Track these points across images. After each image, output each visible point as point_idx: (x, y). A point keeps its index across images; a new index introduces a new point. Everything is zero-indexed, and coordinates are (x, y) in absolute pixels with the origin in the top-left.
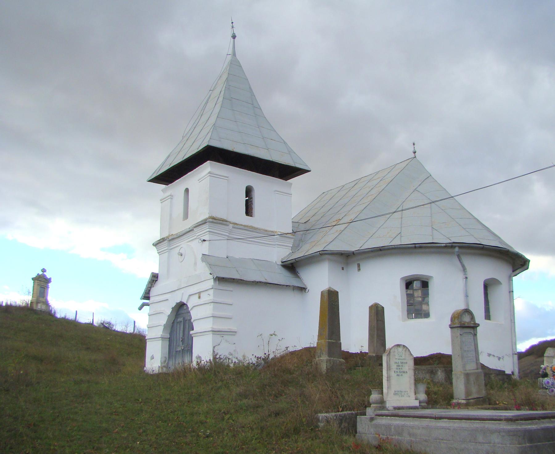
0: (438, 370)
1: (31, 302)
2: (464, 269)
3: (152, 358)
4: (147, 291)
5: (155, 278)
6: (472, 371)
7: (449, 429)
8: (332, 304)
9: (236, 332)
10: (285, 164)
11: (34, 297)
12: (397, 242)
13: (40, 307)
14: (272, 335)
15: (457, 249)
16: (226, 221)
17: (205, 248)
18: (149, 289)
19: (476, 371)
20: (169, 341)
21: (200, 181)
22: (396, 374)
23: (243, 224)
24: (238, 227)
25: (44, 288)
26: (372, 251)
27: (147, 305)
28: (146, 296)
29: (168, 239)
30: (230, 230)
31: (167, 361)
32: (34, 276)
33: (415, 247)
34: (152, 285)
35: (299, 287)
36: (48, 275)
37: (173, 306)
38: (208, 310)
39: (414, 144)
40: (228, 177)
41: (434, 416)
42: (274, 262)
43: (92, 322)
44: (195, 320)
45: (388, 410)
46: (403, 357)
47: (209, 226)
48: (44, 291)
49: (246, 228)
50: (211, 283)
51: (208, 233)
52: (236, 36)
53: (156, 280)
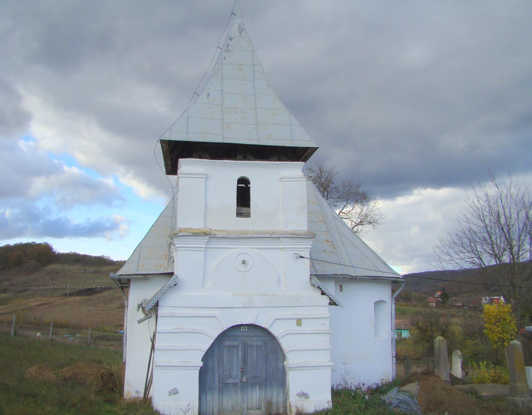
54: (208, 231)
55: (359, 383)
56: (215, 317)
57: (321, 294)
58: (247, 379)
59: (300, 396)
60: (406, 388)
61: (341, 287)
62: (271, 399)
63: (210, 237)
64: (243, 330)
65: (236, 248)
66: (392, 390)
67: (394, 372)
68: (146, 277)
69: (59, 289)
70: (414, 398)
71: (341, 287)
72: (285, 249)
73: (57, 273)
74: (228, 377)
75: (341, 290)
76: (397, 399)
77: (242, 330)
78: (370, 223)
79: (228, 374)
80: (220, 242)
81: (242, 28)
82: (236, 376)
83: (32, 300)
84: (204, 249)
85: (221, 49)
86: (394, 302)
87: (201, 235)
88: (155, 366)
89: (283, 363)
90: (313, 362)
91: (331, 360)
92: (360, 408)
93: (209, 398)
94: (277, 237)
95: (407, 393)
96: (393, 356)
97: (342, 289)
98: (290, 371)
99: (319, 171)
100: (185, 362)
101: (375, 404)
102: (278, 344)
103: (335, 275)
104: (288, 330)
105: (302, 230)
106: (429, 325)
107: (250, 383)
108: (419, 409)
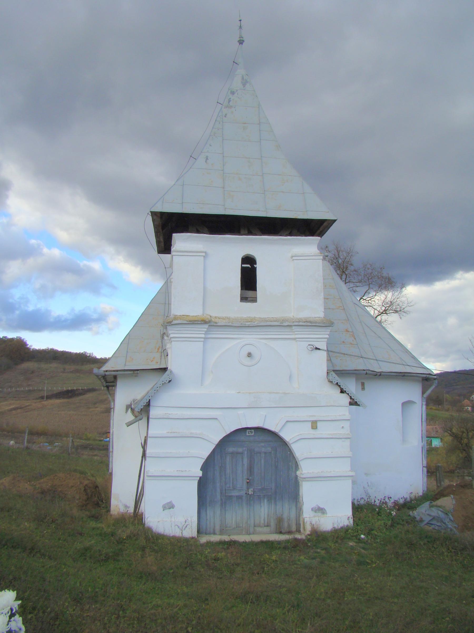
54: (208, 318)
55: (385, 497)
56: (216, 419)
57: (340, 392)
58: (254, 492)
59: (315, 511)
60: (440, 502)
61: (363, 384)
62: (282, 515)
63: (209, 326)
64: (249, 434)
65: (240, 338)
66: (423, 505)
67: (424, 485)
68: (135, 373)
69: (34, 391)
70: (448, 514)
71: (363, 384)
72: (297, 340)
73: (33, 372)
74: (231, 488)
75: (363, 389)
76: (428, 515)
77: (247, 434)
78: (396, 312)
79: (231, 485)
81: (246, 79)
82: (241, 487)
83: (4, 403)
84: (203, 340)
85: (222, 104)
86: (425, 402)
87: (199, 323)
88: (147, 476)
89: (295, 473)
90: (331, 472)
91: (352, 470)
92: (386, 525)
93: (210, 512)
94: (288, 326)
95: (441, 508)
96: (423, 466)
97: (364, 387)
98: (304, 482)
99: (336, 251)
100: (182, 471)
101: (403, 521)
102: (290, 450)
103: (356, 370)
104: (301, 434)
105: (318, 317)
106: (465, 430)
107: (258, 495)
108: (455, 527)
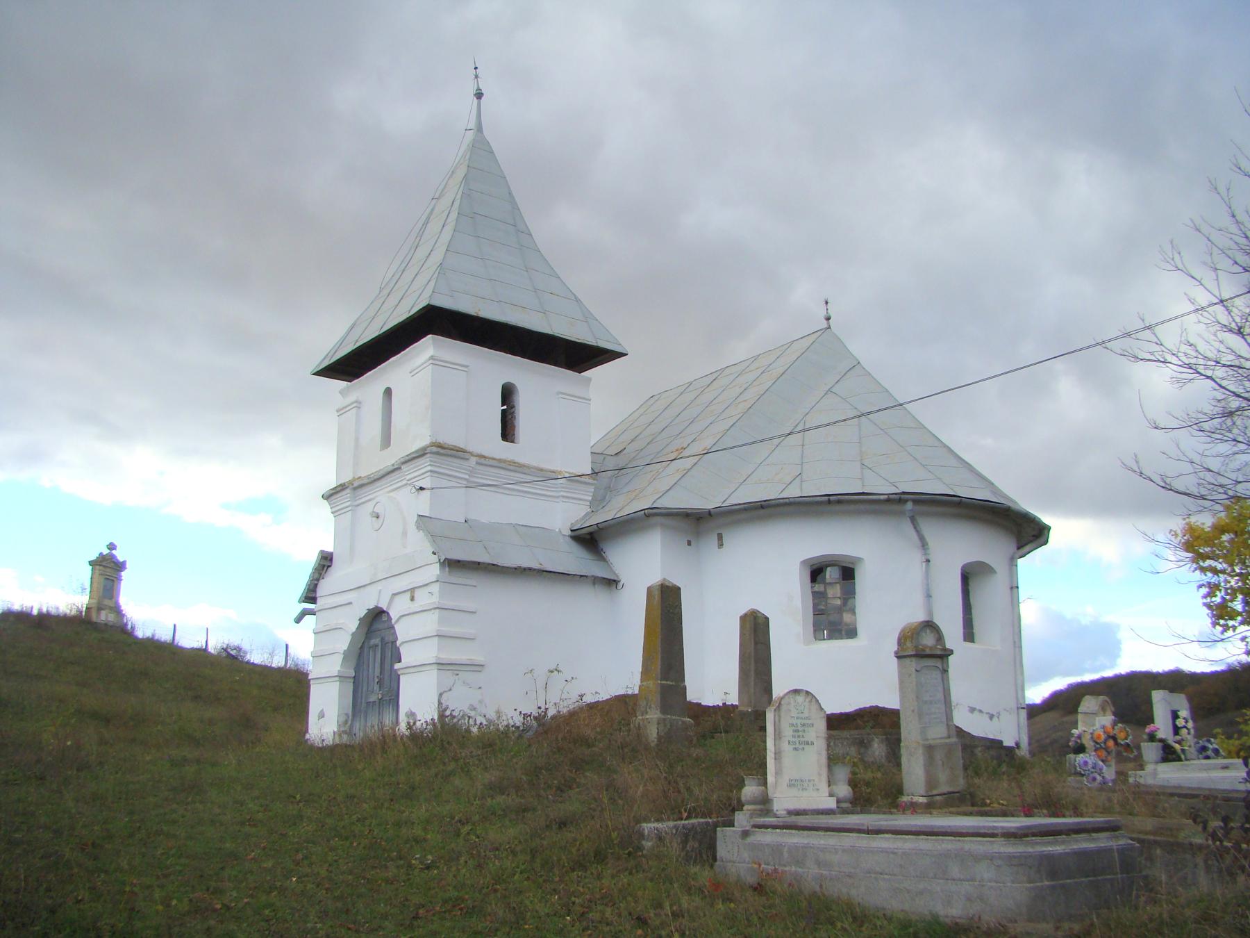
0: (873, 740)
1: (87, 608)
2: (924, 545)
3: (321, 715)
4: (312, 587)
5: (326, 562)
6: (939, 741)
7: (895, 853)
8: (669, 611)
9: (482, 666)
10: (577, 341)
11: (93, 599)
12: (793, 492)
13: (105, 617)
14: (552, 672)
15: (909, 506)
16: (464, 451)
17: (423, 504)
18: (316, 582)
19: (947, 741)
20: (354, 682)
21: (412, 374)
22: (791, 747)
23: (497, 457)
24: (487, 462)
25: (113, 580)
26: (745, 510)
27: (312, 613)
28: (310, 595)
29: (351, 487)
30: (471, 469)
31: (350, 723)
32: (94, 556)
33: (829, 502)
34: (321, 574)
35: (604, 578)
36: (120, 555)
37: (362, 616)
38: (430, 623)
39: (827, 303)
40: (467, 366)
41: (865, 828)
42: (557, 530)
43: (204, 647)
44: (403, 643)
45: (776, 816)
46: (806, 714)
47: (431, 461)
48: (113, 585)
49: (501, 465)
50: (435, 570)
51: (429, 474)
52: (482, 94)
53: (329, 564)
56: (351, 603)
80: (366, 493)
